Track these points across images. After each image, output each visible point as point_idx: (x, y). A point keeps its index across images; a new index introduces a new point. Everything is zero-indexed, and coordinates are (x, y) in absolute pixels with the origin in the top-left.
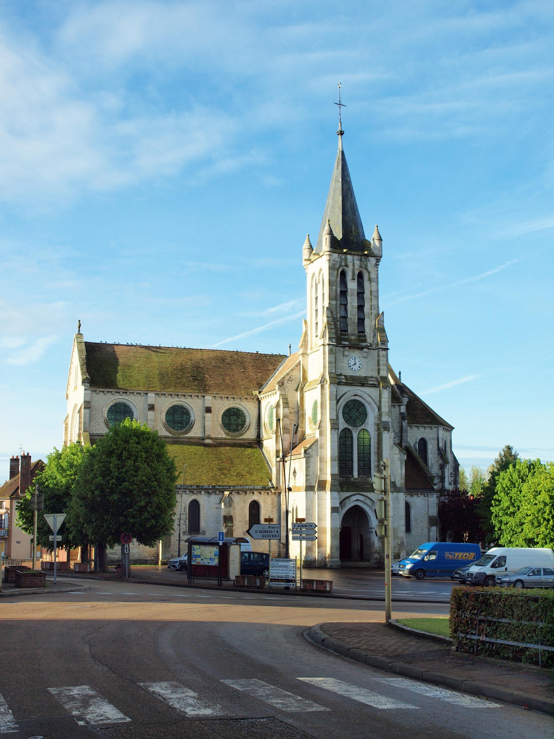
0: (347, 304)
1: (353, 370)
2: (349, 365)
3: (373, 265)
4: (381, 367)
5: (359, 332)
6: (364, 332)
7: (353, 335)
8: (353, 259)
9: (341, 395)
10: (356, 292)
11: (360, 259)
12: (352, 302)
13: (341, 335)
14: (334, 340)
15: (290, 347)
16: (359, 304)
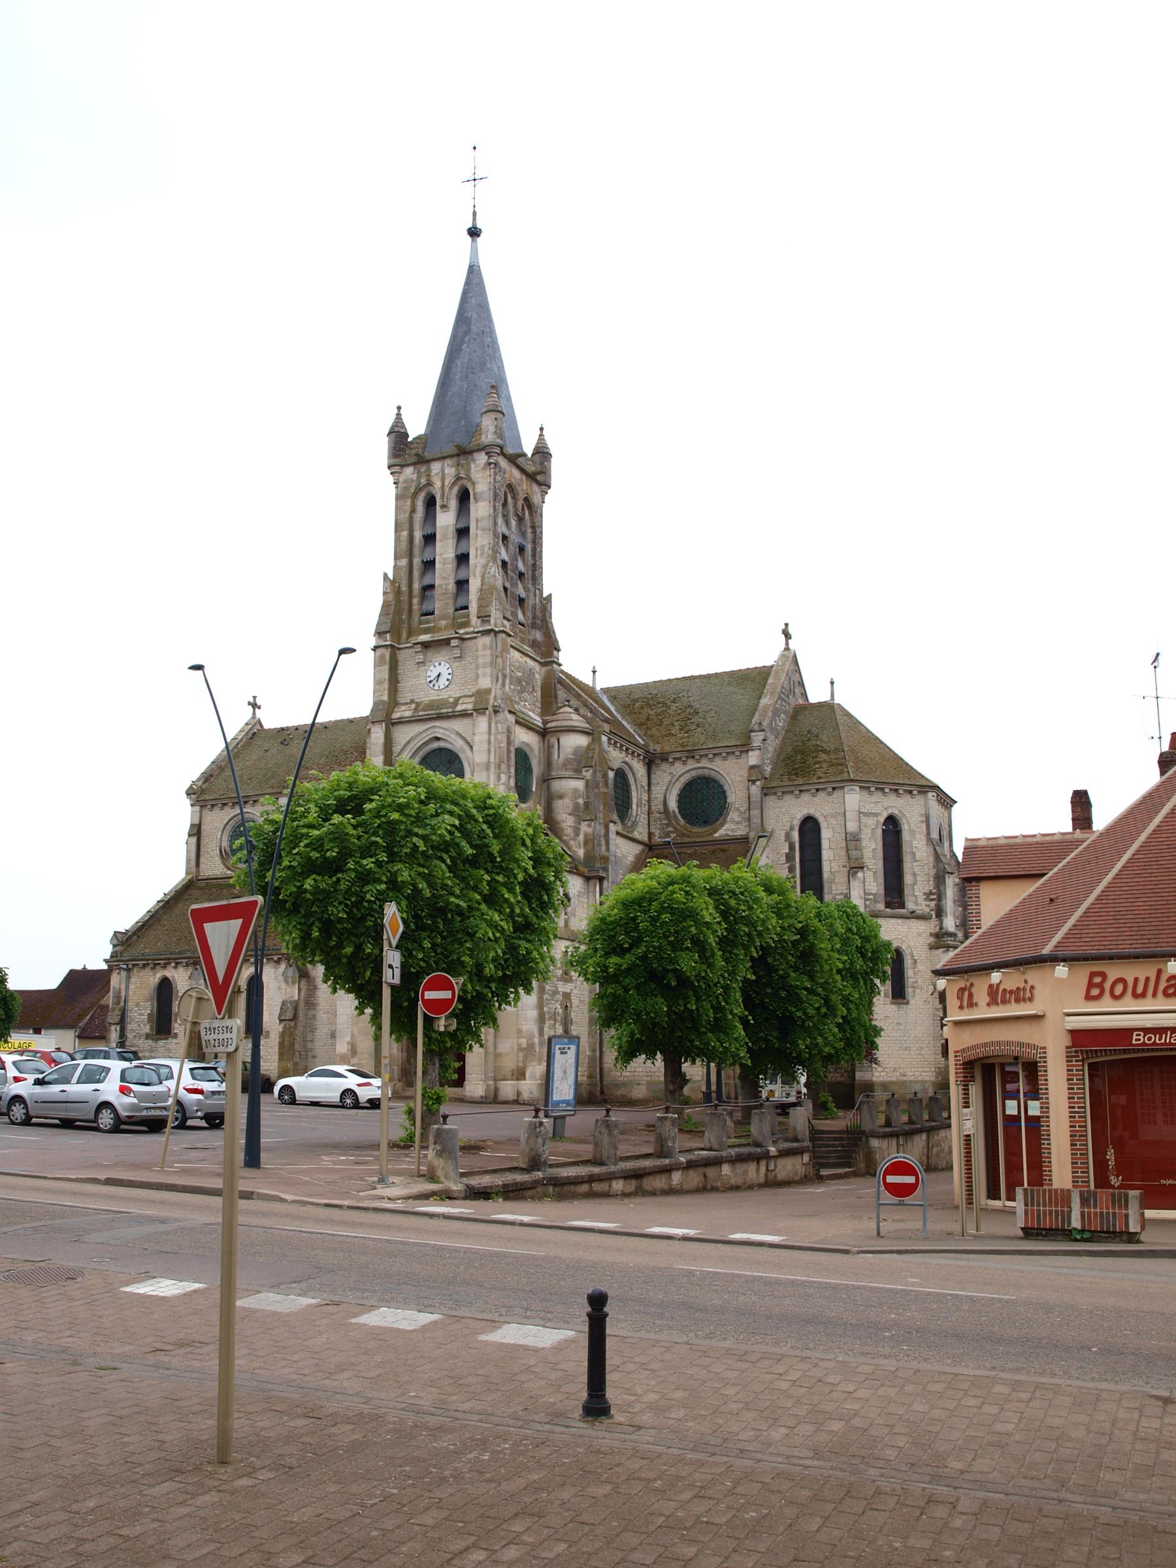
0: (434, 559)
1: (436, 688)
2: (429, 679)
3: (482, 466)
4: (480, 671)
5: (456, 610)
6: (466, 608)
7: (443, 617)
8: (443, 466)
9: (404, 742)
10: (451, 531)
11: (456, 463)
12: (445, 551)
13: (421, 623)
14: (388, 636)
15: (594, 672)
16: (459, 552)
